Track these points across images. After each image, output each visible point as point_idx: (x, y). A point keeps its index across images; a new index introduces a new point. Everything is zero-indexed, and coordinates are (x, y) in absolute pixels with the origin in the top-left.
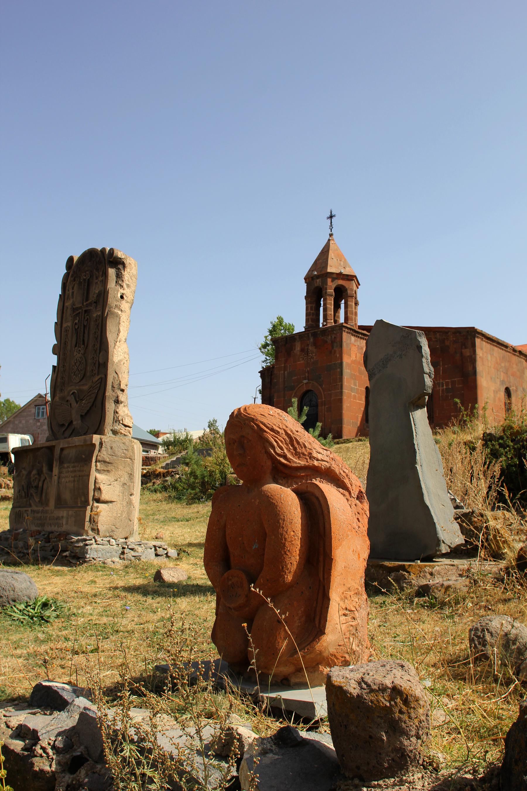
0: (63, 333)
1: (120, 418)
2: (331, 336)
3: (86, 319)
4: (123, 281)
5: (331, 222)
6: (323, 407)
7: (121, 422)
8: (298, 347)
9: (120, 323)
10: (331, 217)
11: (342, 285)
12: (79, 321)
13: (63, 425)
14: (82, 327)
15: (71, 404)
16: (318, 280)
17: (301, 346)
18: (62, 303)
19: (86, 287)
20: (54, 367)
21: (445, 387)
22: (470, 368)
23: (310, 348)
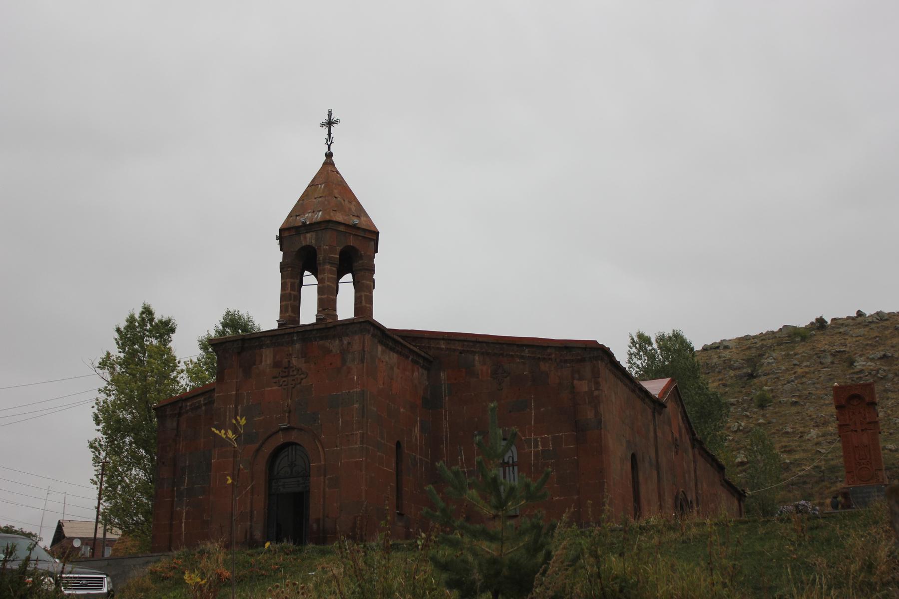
2: (341, 341)
5: (330, 134)
8: (267, 357)
10: (330, 123)
11: (353, 247)
16: (308, 235)
17: (274, 357)
21: (540, 448)
22: (590, 415)
23: (294, 361)
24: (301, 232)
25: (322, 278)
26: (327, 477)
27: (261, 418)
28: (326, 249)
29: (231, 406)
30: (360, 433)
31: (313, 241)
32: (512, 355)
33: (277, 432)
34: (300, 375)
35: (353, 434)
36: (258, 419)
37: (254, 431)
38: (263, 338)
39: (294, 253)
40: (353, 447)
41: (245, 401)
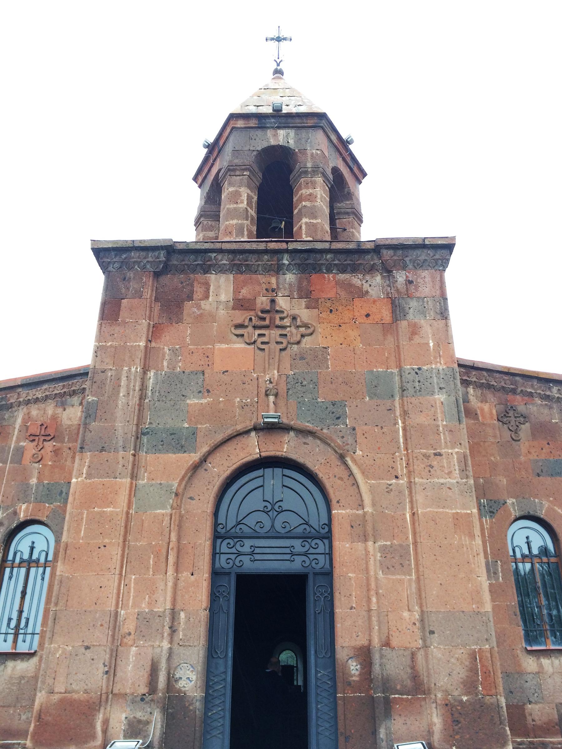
6: (370, 543)
16: (282, 133)
17: (236, 291)
23: (282, 303)
24: (268, 125)
25: (310, 195)
26: (377, 545)
27: (204, 401)
28: (317, 154)
29: (133, 369)
30: (457, 453)
31: (291, 142)
32: (531, 392)
33: (247, 432)
34: (298, 327)
35: (440, 455)
37: (186, 425)
38: (213, 255)
39: (255, 153)
40: (442, 481)
41: (165, 364)
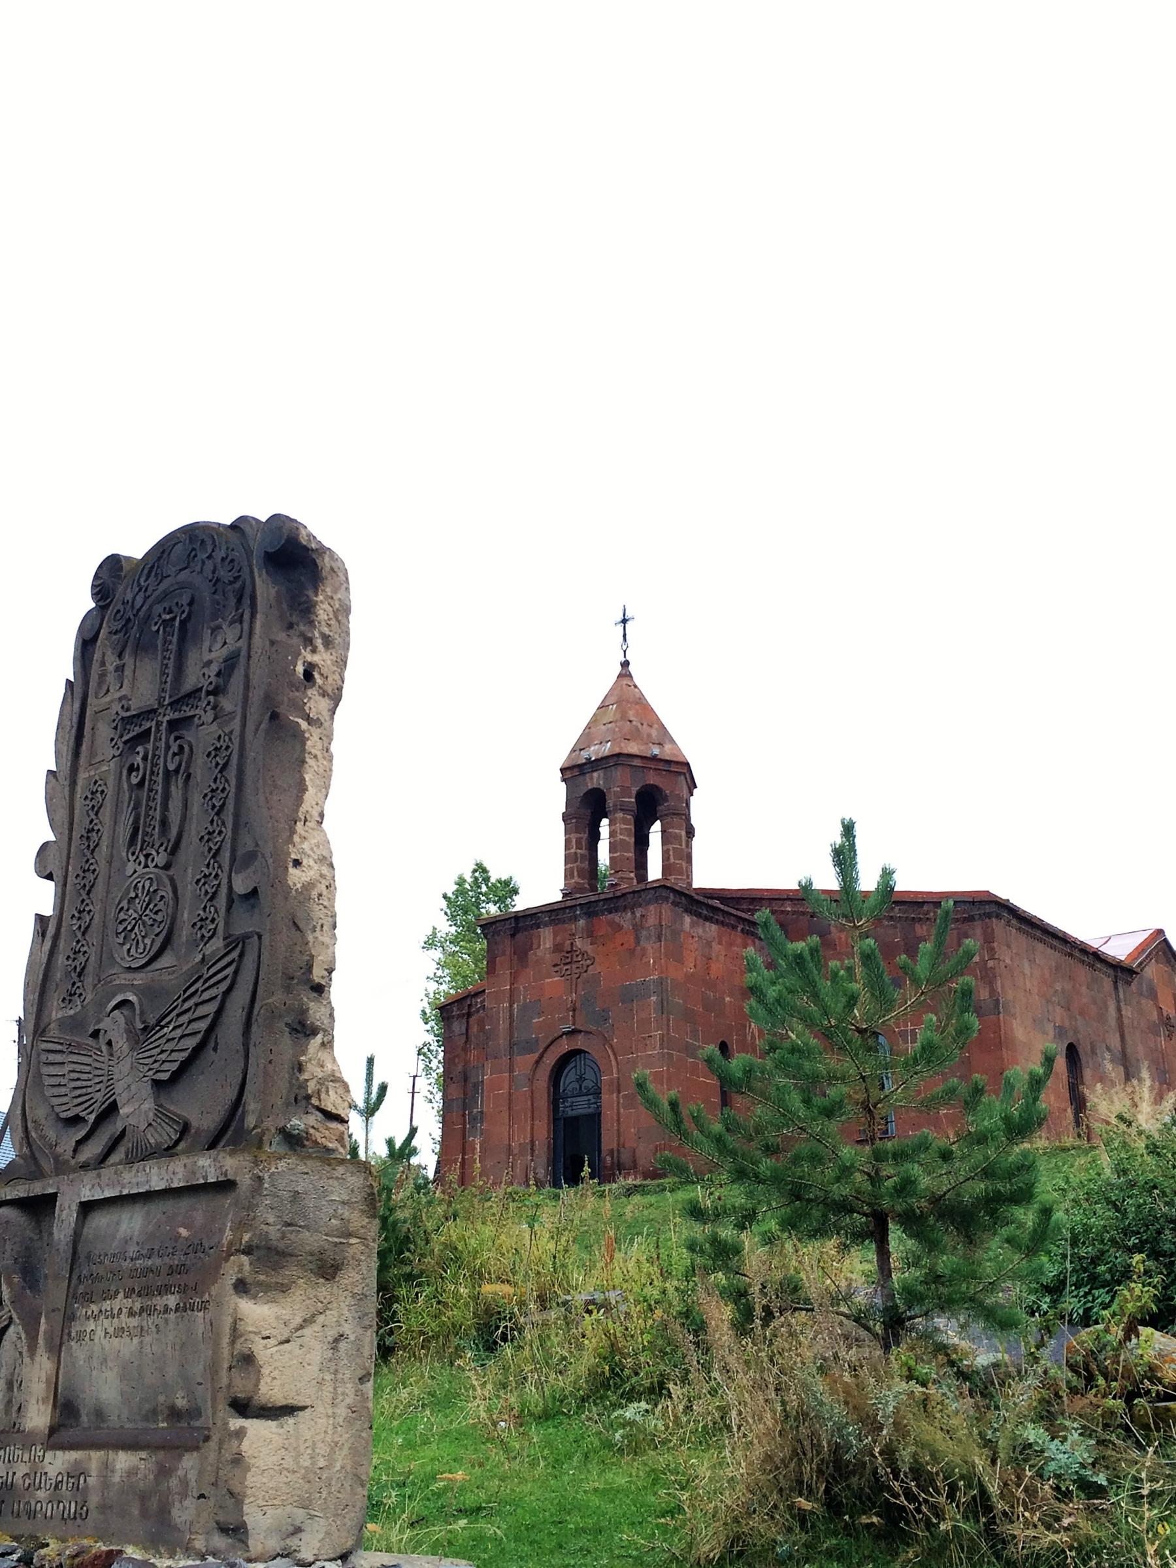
0: (79, 802)
1: (311, 1087)
2: (633, 913)
3: (175, 748)
4: (311, 623)
7: (314, 1101)
9: (303, 762)
12: (145, 758)
13: (76, 1120)
14: (160, 779)
15: (109, 1043)
18: (77, 705)
19: (173, 647)
20: (41, 920)
23: (578, 943)
36: (537, 1020)
